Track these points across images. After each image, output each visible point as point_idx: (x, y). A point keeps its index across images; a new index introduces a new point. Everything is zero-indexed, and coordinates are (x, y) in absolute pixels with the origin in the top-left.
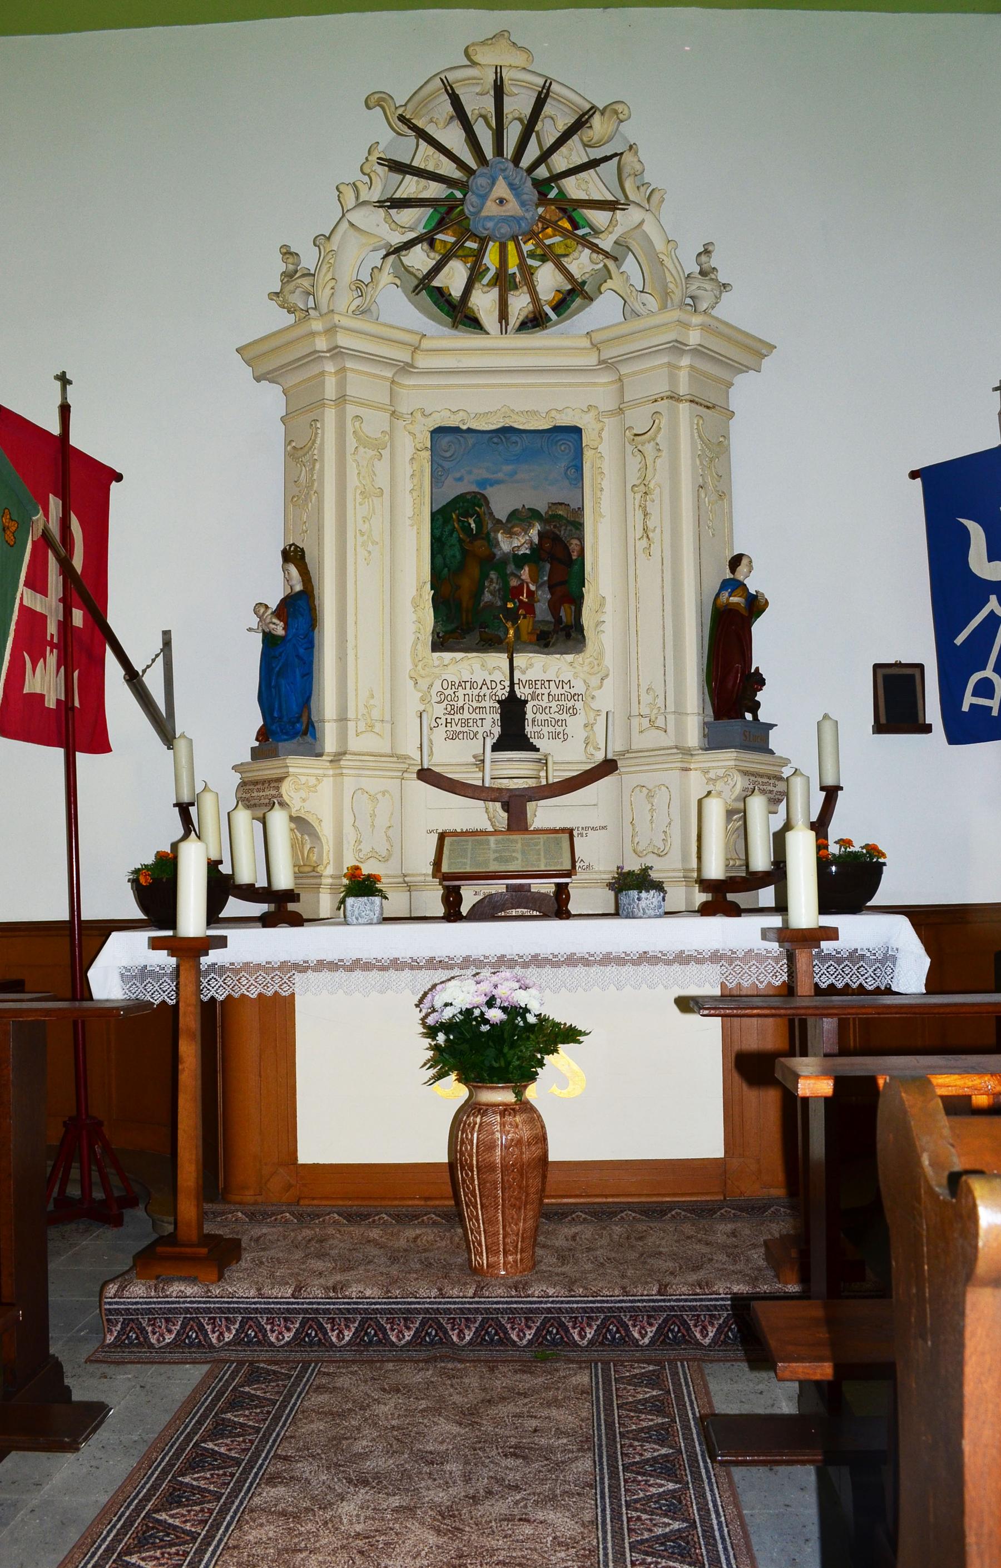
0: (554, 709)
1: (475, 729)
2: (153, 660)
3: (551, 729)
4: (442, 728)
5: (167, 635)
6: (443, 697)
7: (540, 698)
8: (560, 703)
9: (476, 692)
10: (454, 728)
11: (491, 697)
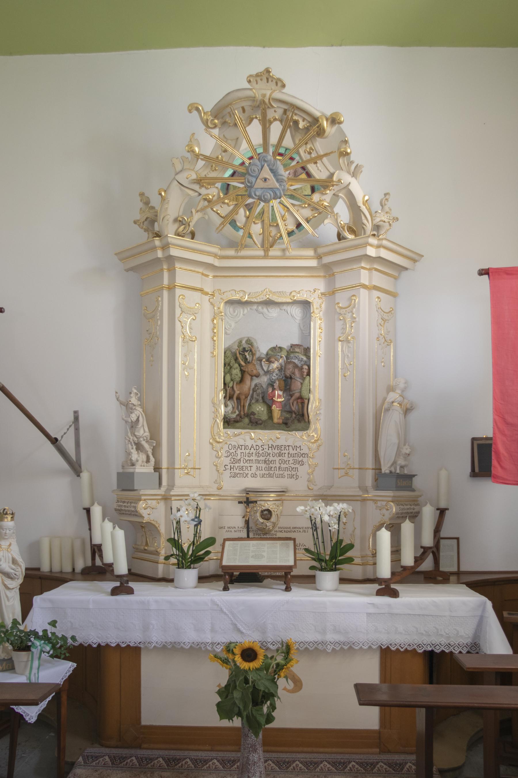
0: (291, 462)
1: (247, 472)
2: (68, 429)
3: (289, 473)
4: (228, 471)
5: (76, 412)
6: (229, 454)
7: (283, 455)
8: (295, 458)
9: (247, 451)
10: (235, 471)
11: (256, 454)
